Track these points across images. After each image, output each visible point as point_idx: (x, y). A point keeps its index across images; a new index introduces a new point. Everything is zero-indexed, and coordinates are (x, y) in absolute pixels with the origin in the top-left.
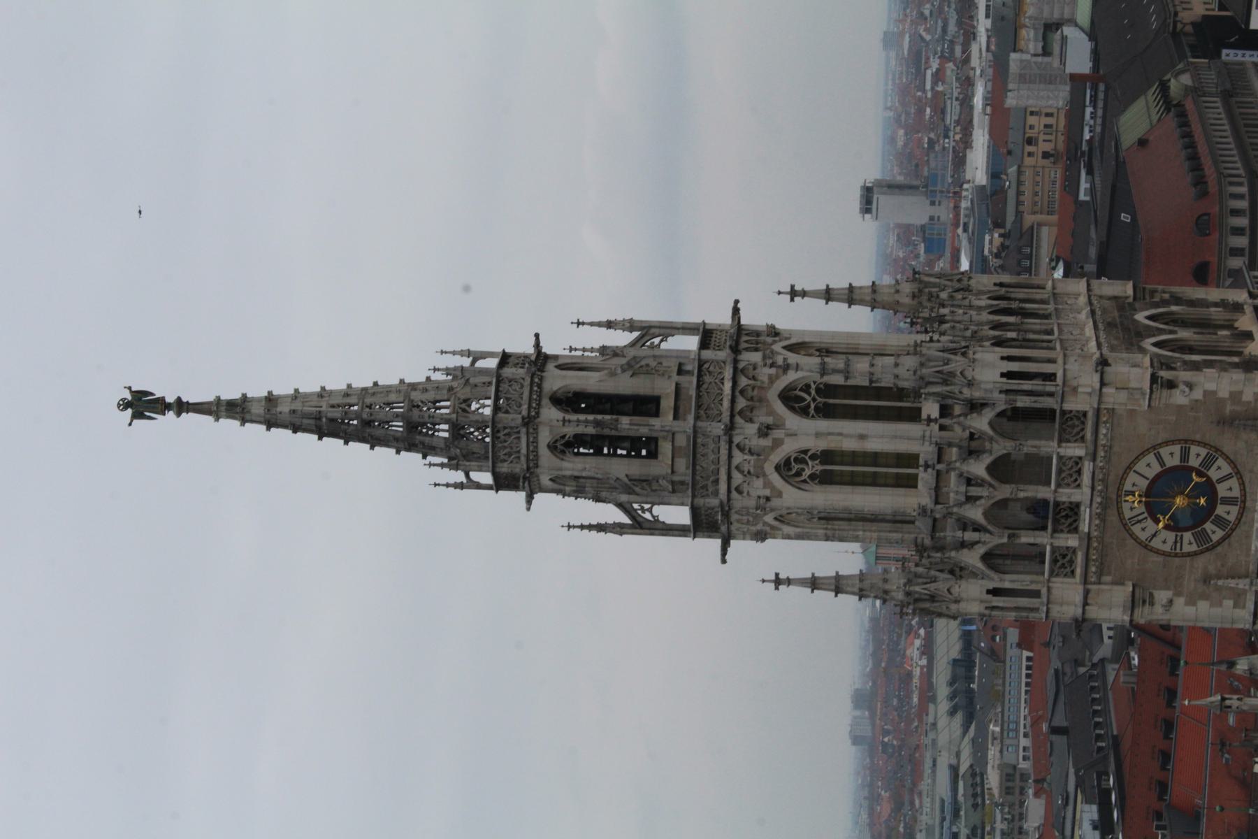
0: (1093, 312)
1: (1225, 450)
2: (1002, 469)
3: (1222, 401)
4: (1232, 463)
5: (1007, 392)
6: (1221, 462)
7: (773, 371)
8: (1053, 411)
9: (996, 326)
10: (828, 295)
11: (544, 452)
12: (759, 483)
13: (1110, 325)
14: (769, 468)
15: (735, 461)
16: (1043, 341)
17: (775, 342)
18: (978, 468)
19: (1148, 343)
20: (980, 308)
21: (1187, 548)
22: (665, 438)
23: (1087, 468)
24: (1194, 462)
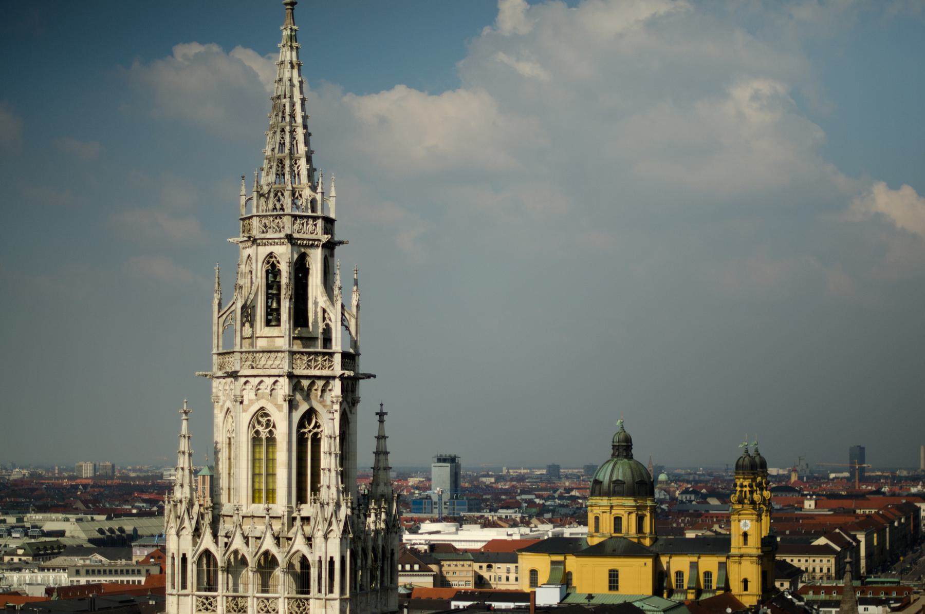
5: (320, 561)
8: (308, 593)
9: (364, 551)
10: (381, 438)
11: (269, 249)
12: (252, 395)
14: (262, 403)
17: (348, 403)
18: (269, 544)
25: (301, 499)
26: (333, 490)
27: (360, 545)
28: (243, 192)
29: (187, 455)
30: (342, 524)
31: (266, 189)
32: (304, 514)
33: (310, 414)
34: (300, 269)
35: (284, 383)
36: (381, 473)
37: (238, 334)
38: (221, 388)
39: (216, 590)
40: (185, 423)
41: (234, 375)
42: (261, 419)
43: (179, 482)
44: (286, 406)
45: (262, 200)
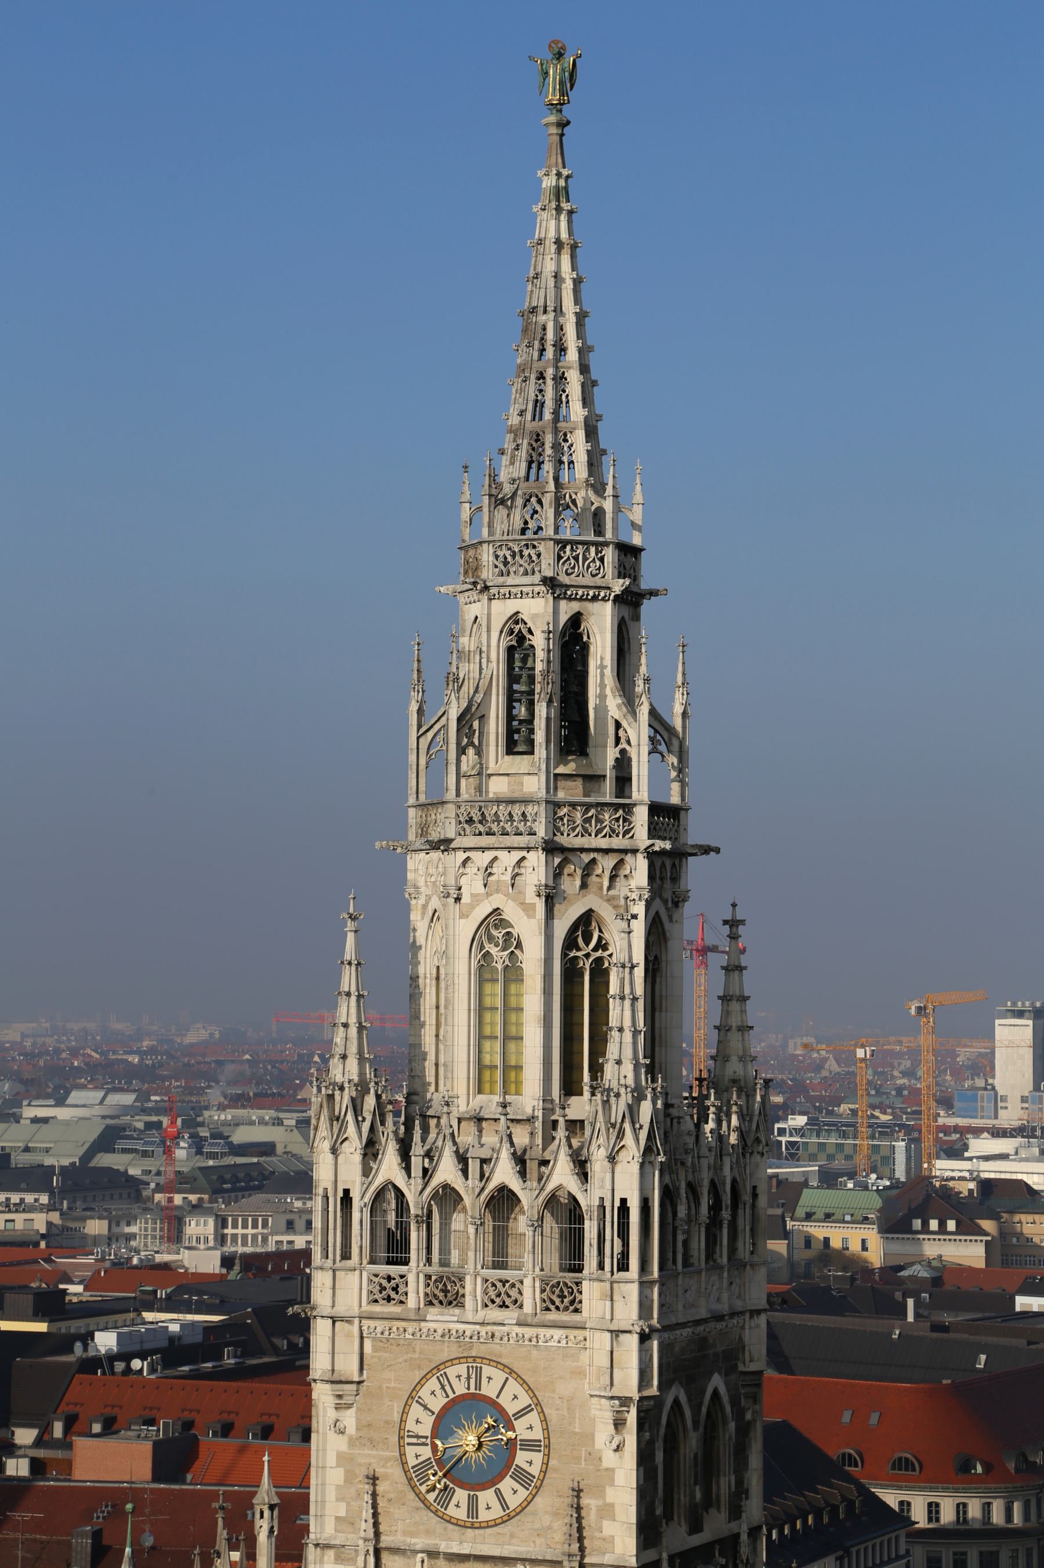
0: (719, 1318)
1: (537, 1499)
2: (503, 1202)
3: (602, 1494)
4: (522, 1508)
5: (602, 1207)
6: (523, 1493)
7: (622, 902)
8: (580, 1270)
11: (511, 606)
13: (702, 1342)
14: (497, 901)
15: (502, 855)
16: (674, 1253)
17: (665, 902)
18: (505, 1173)
19: (678, 1392)
20: (717, 1168)
21: (410, 1451)
22: (533, 764)
23: (510, 1315)
24: (522, 1458)
25: (570, 1087)
26: (628, 1068)
27: (682, 1177)
28: (467, 496)
29: (353, 999)
30: (643, 1135)
31: (508, 489)
32: (573, 1114)
33: (585, 922)
34: (572, 642)
35: (536, 859)
36: (734, 1037)
37: (452, 768)
38: (422, 869)
39: (406, 1262)
40: (351, 938)
41: (444, 845)
42: (495, 933)
43: (339, 1050)
44: (540, 906)
45: (502, 511)
